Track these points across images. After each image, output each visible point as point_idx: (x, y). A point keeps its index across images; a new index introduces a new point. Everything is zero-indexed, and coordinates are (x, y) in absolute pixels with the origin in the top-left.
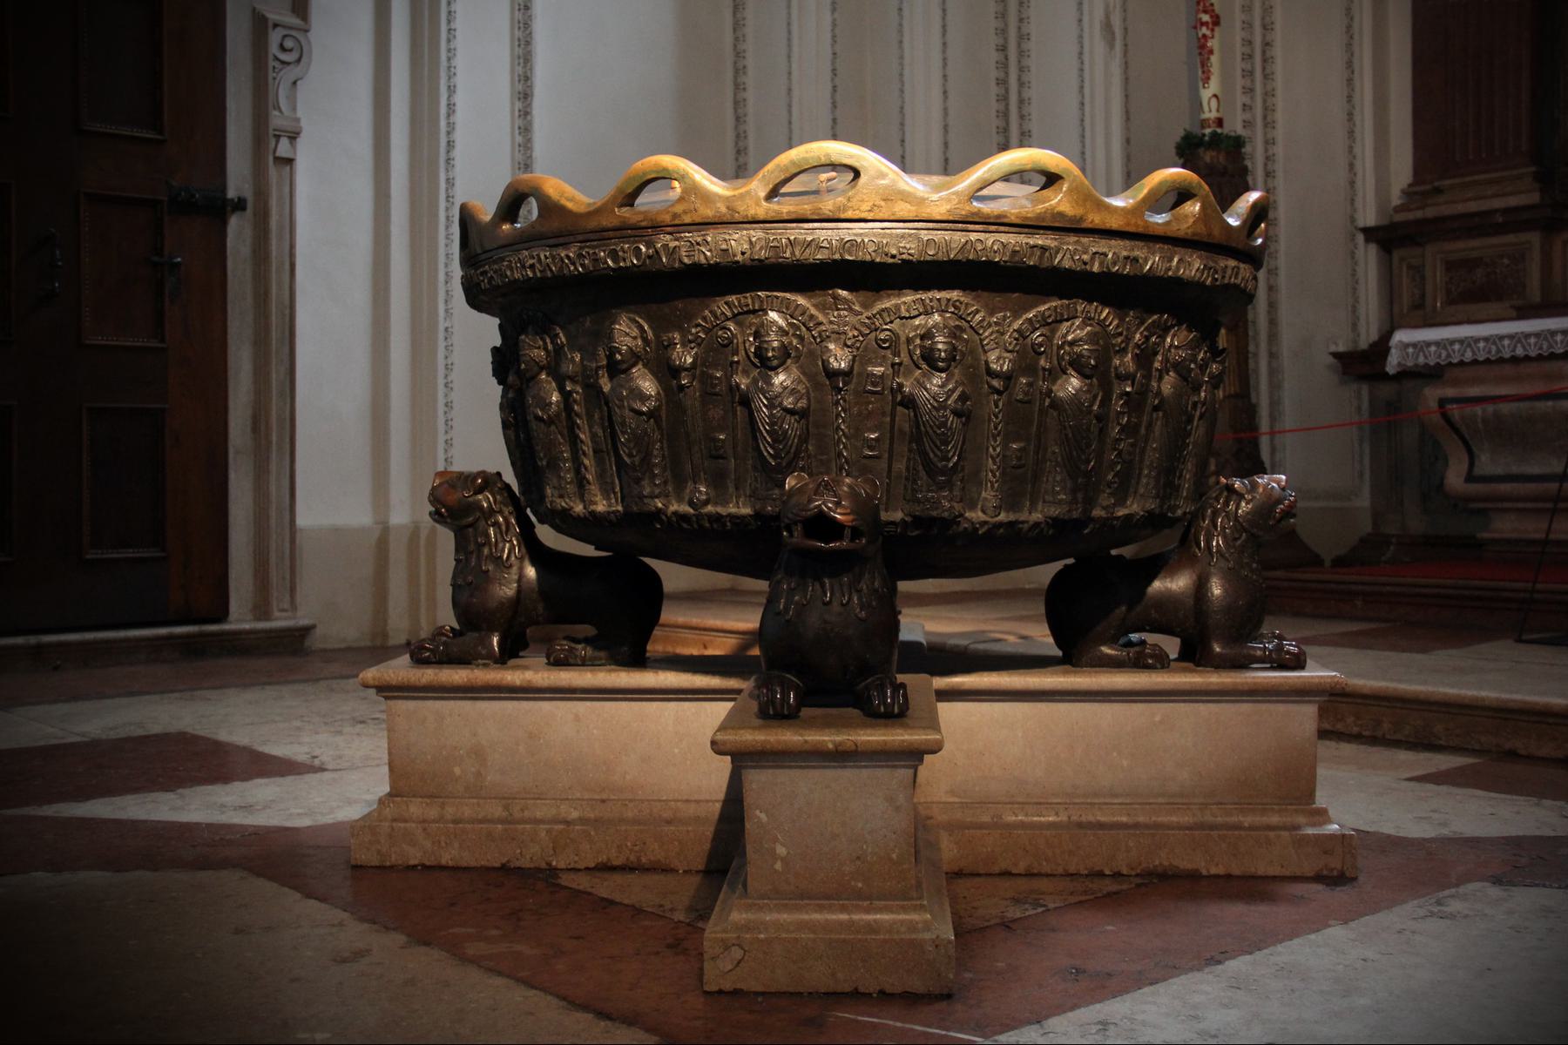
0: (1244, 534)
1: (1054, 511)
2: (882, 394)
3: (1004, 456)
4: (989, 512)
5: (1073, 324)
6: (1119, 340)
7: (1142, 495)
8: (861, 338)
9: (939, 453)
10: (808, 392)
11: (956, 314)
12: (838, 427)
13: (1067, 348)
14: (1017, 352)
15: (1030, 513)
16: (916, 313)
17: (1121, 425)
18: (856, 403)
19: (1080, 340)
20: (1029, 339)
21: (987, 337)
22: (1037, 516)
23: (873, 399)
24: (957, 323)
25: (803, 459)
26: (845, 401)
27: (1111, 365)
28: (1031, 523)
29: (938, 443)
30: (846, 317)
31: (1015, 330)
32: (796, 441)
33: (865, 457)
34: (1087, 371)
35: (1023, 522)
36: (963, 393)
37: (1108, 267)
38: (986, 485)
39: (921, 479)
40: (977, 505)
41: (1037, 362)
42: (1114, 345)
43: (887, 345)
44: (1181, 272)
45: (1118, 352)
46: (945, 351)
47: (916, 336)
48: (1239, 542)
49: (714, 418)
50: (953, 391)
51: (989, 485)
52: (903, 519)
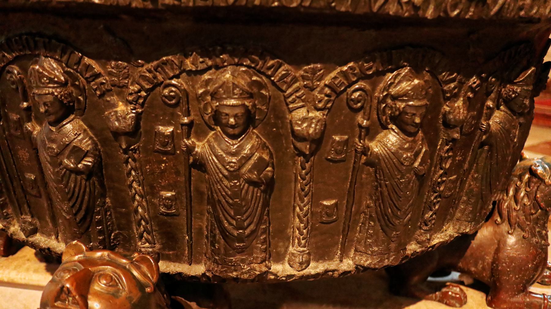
0: (540, 211)
1: (366, 261)
2: (174, 154)
3: (312, 213)
4: (295, 266)
5: (399, 74)
6: (452, 85)
7: (458, 220)
8: (143, 94)
9: (234, 222)
10: (95, 147)
11: (253, 68)
12: (131, 186)
13: (389, 101)
14: (329, 109)
15: (341, 261)
16: (204, 66)
17: (445, 169)
18: (148, 162)
19: (406, 94)
20: (344, 96)
21: (291, 94)
22: (347, 265)
23: (165, 158)
24: (254, 78)
25: (98, 213)
26: (134, 160)
27: (440, 111)
28: (341, 272)
29: (232, 213)
30: (125, 68)
31: (326, 85)
32: (86, 197)
33: (162, 214)
34: (412, 129)
35: (333, 271)
36: (260, 159)
37: (446, 12)
38: (293, 240)
39: (219, 243)
40: (285, 257)
41: (353, 119)
42: (444, 92)
43: (174, 102)
44: (534, 11)
45: (448, 99)
46: (235, 116)
47: (206, 93)
48: (535, 216)
49: (23, 158)
50: (248, 158)
51: (296, 241)
52: (204, 275)
